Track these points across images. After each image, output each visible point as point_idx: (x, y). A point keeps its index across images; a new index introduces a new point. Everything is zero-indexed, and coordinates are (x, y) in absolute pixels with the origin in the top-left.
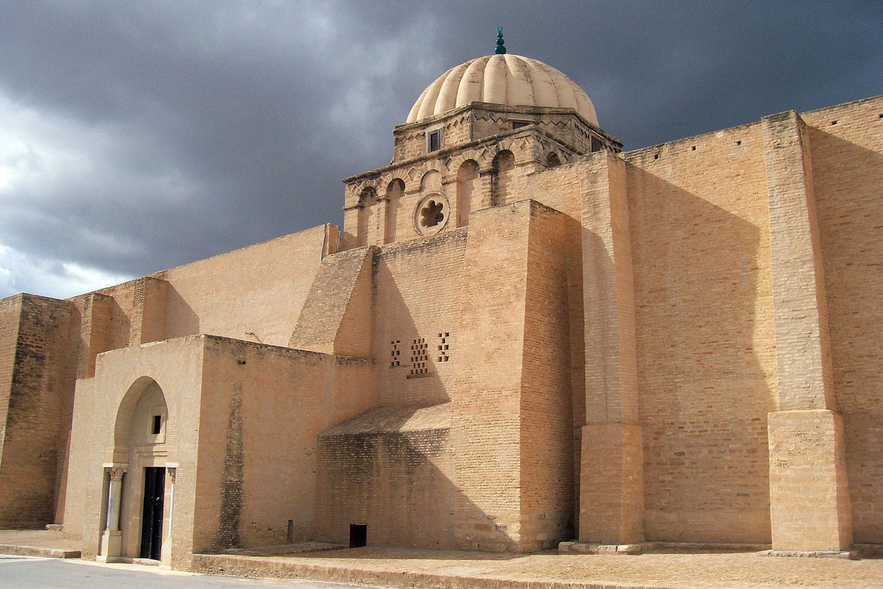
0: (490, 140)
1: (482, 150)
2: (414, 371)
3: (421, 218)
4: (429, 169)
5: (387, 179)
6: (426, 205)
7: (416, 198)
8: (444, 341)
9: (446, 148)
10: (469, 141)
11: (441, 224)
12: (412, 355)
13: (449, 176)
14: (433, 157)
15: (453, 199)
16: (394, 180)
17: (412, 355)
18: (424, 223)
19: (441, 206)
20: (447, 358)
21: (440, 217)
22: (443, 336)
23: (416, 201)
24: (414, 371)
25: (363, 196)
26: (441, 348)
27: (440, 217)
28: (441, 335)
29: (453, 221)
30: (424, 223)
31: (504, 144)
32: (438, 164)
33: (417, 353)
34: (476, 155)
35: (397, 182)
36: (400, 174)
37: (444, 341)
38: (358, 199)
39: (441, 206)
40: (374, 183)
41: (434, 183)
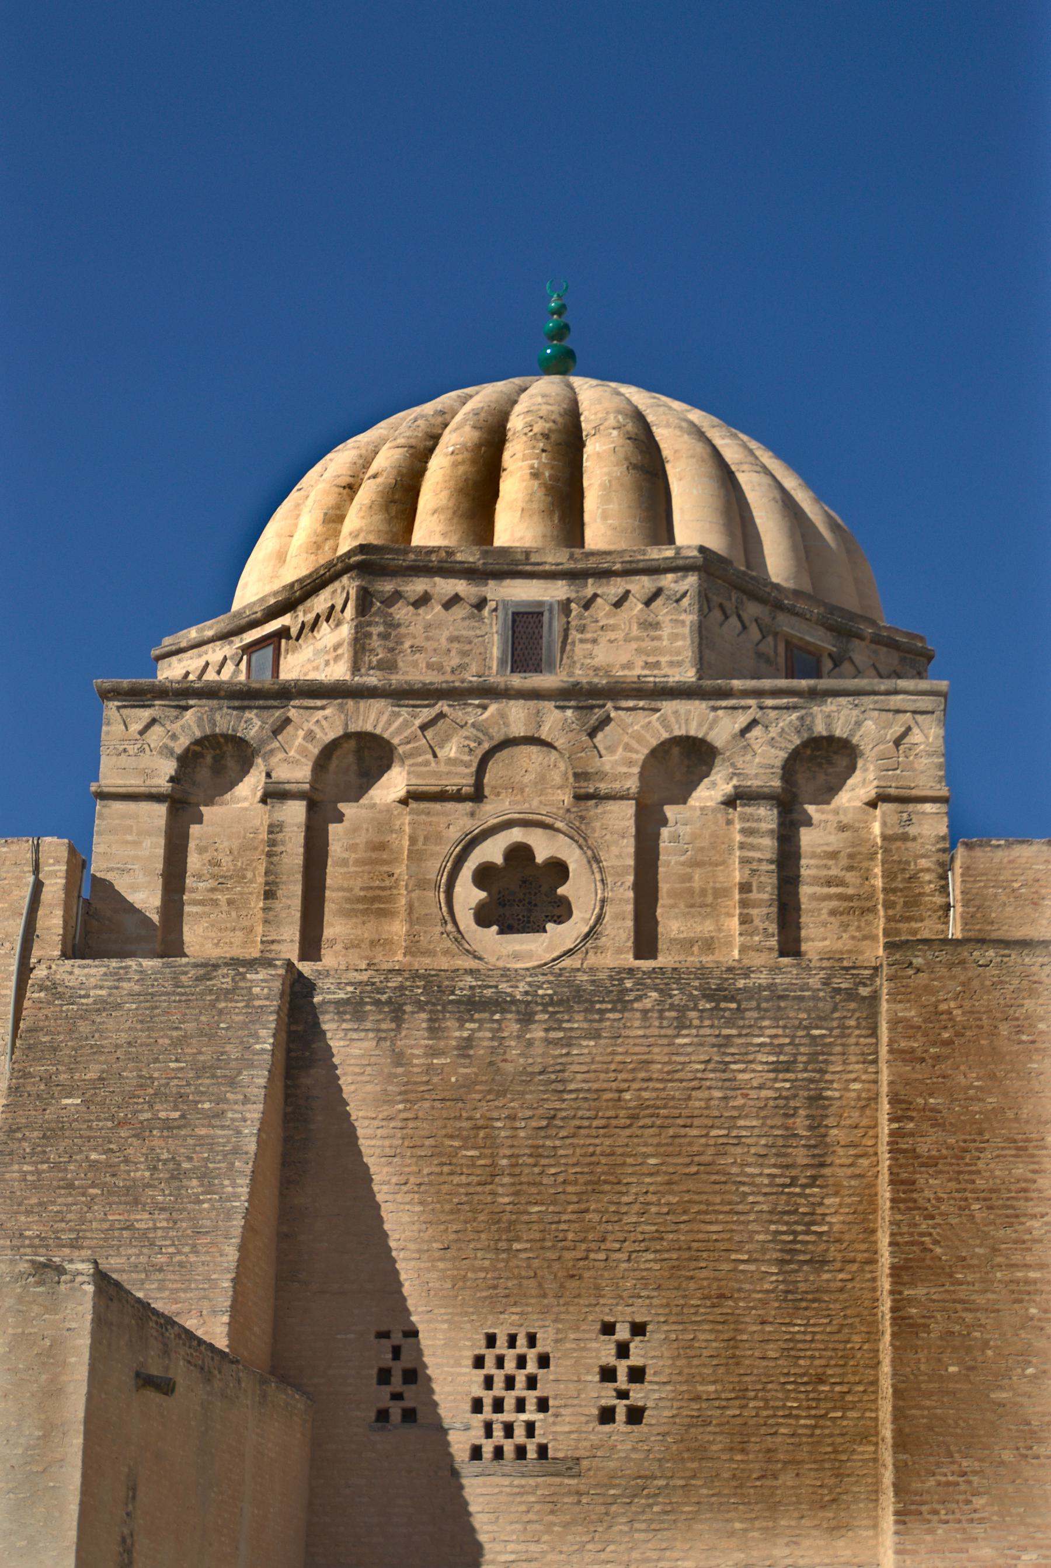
0: (776, 693)
1: (742, 719)
2: (488, 1451)
3: (469, 895)
4: (518, 729)
5: (326, 723)
6: (492, 851)
7: (457, 821)
8: (623, 1351)
9: (581, 676)
10: (688, 675)
11: (560, 936)
12: (478, 1390)
13: (601, 775)
14: (535, 695)
15: (621, 853)
16: (347, 736)
17: (478, 1390)
18: (483, 917)
19: (559, 870)
20: (635, 1415)
21: (562, 911)
22: (623, 1333)
23: (454, 833)
24: (488, 1451)
25: (188, 760)
26: (608, 1374)
27: (562, 911)
28: (608, 1329)
29: (620, 930)
30: (483, 917)
31: (835, 717)
32: (554, 721)
33: (499, 1383)
34: (718, 725)
35: (352, 744)
37: (623, 1351)
38: (168, 767)
39: (559, 870)
40: (252, 725)
41: (532, 783)
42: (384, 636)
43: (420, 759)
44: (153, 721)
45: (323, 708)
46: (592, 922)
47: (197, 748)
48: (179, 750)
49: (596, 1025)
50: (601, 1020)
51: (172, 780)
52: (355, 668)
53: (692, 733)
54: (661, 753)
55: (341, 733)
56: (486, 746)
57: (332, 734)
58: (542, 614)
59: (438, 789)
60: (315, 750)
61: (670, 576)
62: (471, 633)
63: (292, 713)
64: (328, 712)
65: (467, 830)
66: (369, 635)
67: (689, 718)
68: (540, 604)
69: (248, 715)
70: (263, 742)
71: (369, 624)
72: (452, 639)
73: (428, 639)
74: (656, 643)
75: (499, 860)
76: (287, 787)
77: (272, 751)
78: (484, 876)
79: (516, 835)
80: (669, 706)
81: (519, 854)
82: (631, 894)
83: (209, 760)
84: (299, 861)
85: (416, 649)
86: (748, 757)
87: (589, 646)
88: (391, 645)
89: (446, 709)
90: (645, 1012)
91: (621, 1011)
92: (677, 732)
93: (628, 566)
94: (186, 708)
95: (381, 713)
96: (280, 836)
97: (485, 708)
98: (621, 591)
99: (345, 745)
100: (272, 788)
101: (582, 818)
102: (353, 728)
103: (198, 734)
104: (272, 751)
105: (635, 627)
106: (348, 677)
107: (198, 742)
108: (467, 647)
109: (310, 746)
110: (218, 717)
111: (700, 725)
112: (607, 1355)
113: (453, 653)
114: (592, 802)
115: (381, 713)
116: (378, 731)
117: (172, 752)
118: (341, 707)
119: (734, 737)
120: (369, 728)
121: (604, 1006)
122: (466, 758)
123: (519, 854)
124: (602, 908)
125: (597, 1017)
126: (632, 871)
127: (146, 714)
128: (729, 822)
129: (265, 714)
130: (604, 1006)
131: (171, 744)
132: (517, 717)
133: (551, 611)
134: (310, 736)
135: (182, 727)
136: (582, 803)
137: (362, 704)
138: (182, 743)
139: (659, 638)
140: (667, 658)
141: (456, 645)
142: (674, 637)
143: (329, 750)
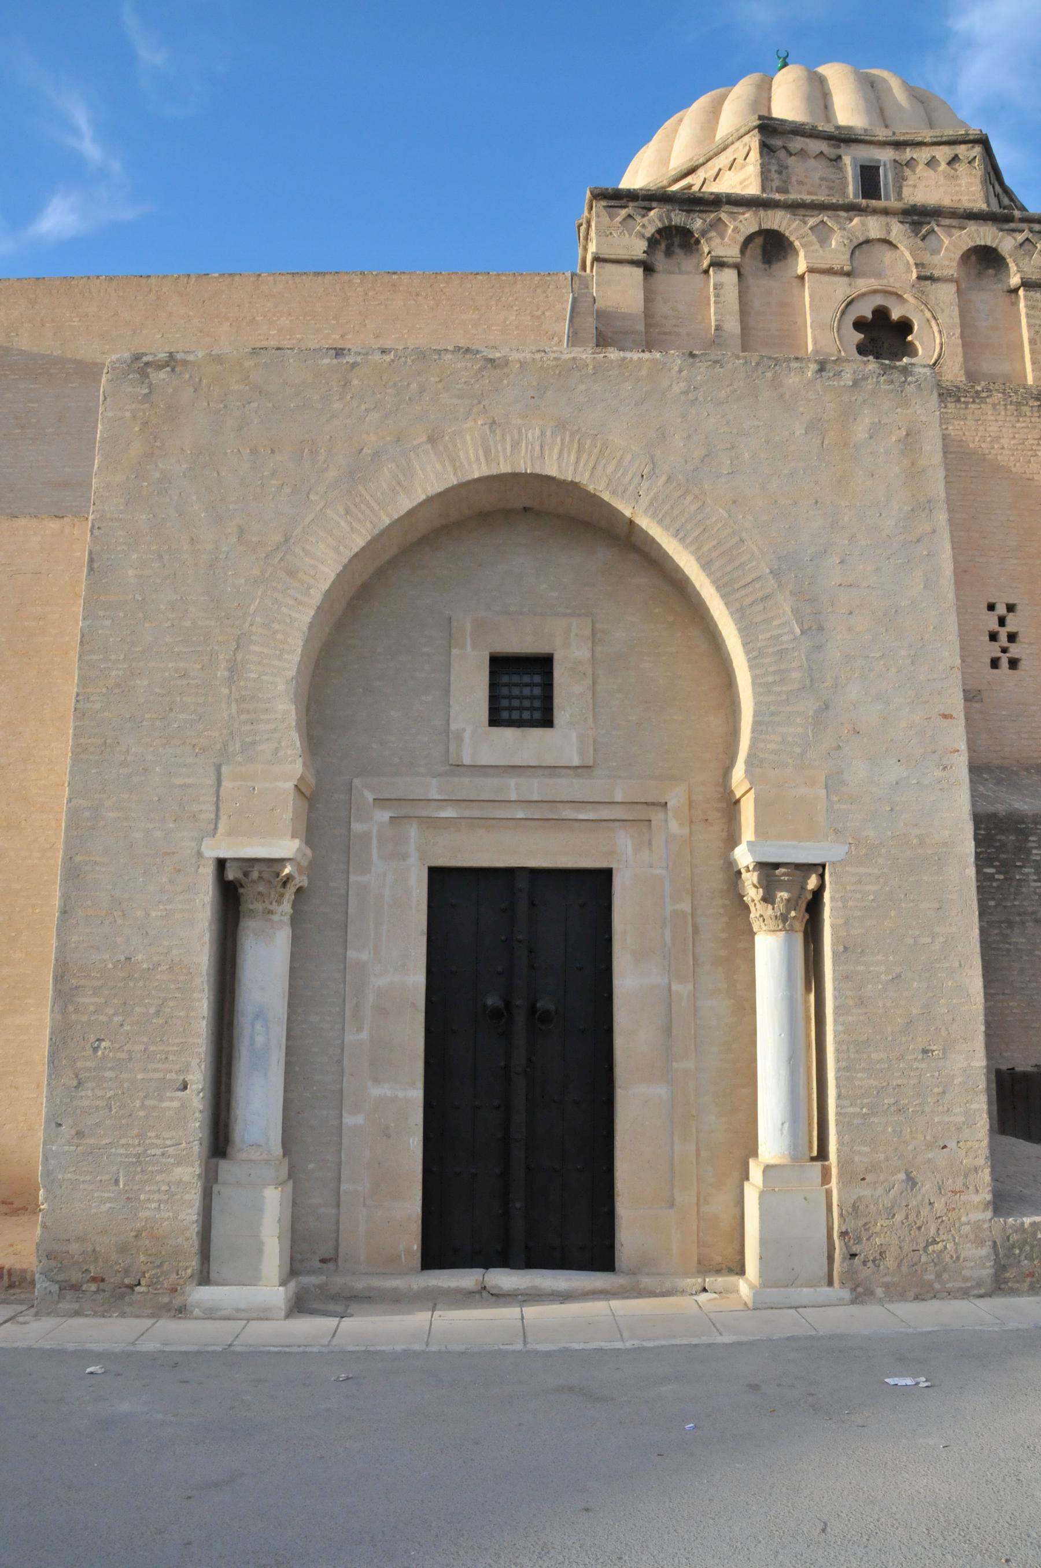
5: (748, 222)
6: (865, 310)
7: (840, 289)
15: (950, 315)
35: (759, 241)
36: (777, 220)
38: (643, 245)
42: (780, 173)
43: (812, 248)
44: (629, 216)
45: (743, 214)
46: (935, 356)
47: (658, 236)
48: (648, 235)
49: (962, 411)
50: (966, 408)
51: (644, 252)
52: (763, 190)
53: (989, 244)
54: (966, 257)
55: (757, 229)
56: (856, 242)
57: (753, 228)
58: (878, 168)
59: (828, 266)
60: (742, 239)
61: (963, 147)
62: (833, 176)
63: (724, 216)
64: (747, 215)
65: (848, 293)
66: (769, 171)
67: (986, 235)
68: (879, 161)
69: (692, 215)
70: (704, 233)
71: (769, 164)
72: (822, 179)
73: (806, 177)
74: (957, 188)
75: (869, 315)
76: (725, 259)
77: (711, 238)
78: (859, 325)
79: (879, 301)
80: (972, 227)
81: (881, 313)
82: (960, 341)
83: (663, 246)
84: (737, 307)
85: (801, 183)
86: (1026, 261)
87: (911, 189)
88: (784, 178)
89: (825, 219)
90: (994, 406)
91: (979, 404)
92: (978, 243)
93: (935, 140)
94: (650, 209)
95: (783, 218)
96: (722, 292)
97: (851, 220)
98: (929, 157)
99: (756, 241)
100: (714, 260)
101: (923, 292)
102: (765, 226)
103: (660, 225)
104: (711, 238)
105: (942, 178)
106: (758, 193)
107: (659, 231)
108: (832, 185)
109: (737, 236)
110: (673, 215)
111: (993, 240)
112: (994, 626)
113: (823, 187)
114: (929, 282)
115: (783, 218)
116: (782, 230)
117: (644, 237)
118: (756, 213)
119: (1016, 248)
120: (776, 227)
121: (967, 400)
122: (843, 249)
123: (881, 313)
124: (941, 348)
125: (963, 406)
126: (958, 326)
127: (624, 212)
128: (1016, 304)
129: (704, 216)
130: (967, 400)
131: (643, 231)
132: (873, 227)
133: (885, 165)
134: (736, 230)
135: (649, 220)
136: (923, 283)
137: (770, 212)
138: (650, 231)
139: (960, 185)
140: (966, 198)
141: (824, 183)
142: (970, 185)
143: (749, 240)
